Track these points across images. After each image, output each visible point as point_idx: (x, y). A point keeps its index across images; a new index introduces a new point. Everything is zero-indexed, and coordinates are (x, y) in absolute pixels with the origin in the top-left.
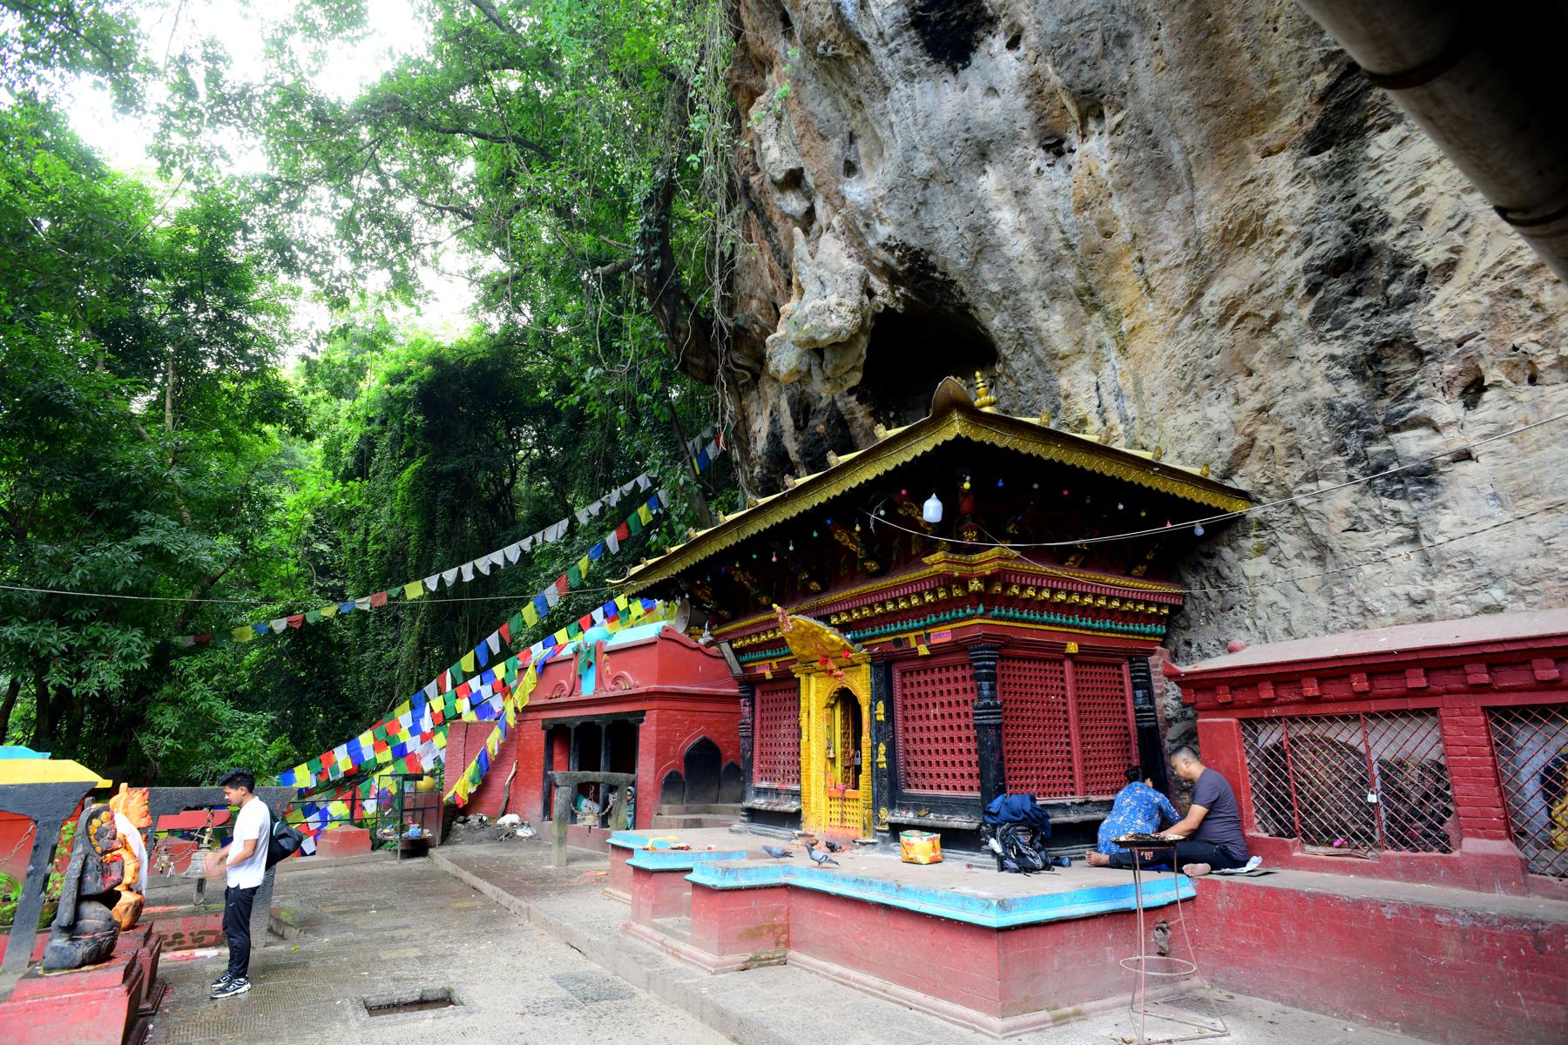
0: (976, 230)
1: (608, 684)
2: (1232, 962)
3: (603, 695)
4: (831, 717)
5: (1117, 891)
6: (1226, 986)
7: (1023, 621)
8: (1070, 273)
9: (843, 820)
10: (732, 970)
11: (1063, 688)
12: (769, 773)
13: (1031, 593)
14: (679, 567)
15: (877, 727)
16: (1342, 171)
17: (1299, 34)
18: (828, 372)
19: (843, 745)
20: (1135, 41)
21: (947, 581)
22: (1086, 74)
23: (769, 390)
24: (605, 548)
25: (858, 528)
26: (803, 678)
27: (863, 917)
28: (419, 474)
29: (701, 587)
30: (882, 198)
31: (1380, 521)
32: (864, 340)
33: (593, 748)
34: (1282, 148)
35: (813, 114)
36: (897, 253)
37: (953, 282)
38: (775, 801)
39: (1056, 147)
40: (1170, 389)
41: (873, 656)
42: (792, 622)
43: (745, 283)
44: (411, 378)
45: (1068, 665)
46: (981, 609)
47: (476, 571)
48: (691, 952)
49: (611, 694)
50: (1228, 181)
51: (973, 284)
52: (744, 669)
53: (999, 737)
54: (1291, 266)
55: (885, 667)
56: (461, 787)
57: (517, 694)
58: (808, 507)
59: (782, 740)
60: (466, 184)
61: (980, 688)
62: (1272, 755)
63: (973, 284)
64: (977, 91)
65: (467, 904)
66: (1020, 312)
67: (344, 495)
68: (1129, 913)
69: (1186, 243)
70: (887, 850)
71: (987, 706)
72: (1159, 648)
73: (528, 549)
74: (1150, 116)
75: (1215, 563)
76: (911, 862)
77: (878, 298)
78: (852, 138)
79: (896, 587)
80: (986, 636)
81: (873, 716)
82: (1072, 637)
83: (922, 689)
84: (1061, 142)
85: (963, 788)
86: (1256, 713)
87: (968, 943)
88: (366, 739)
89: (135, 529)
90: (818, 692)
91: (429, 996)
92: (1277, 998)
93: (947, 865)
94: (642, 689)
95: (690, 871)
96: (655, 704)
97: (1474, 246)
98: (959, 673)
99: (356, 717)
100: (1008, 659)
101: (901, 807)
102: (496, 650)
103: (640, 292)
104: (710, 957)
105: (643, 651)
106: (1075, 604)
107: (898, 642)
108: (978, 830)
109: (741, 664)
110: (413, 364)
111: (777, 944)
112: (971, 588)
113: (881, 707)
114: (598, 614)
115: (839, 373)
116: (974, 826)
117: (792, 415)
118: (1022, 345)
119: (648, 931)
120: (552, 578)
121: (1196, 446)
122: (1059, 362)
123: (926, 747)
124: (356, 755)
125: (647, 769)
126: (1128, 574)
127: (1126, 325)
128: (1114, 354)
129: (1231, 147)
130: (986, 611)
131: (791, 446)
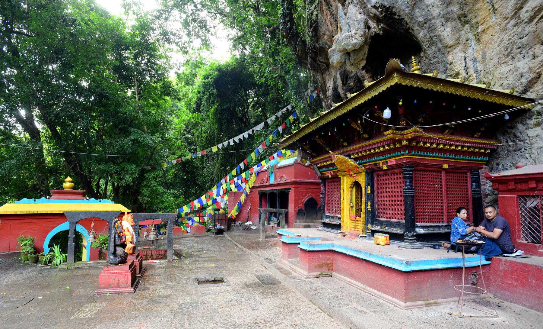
1: (278, 179)
2: (505, 290)
3: (277, 183)
4: (352, 191)
5: (456, 260)
6: (501, 298)
7: (425, 156)
9: (355, 228)
10: (312, 277)
11: (441, 182)
12: (331, 211)
13: (428, 145)
14: (297, 138)
15: (367, 195)
18: (352, 62)
19: (356, 201)
21: (394, 141)
23: (333, 71)
24: (278, 131)
25: (359, 122)
26: (342, 177)
27: (357, 263)
28: (216, 109)
29: (306, 145)
32: (367, 48)
33: (274, 200)
36: (379, 9)
37: (403, 19)
38: (332, 220)
40: (499, 56)
41: (367, 170)
42: (337, 157)
43: (322, 29)
44: (211, 77)
45: (443, 173)
46: (407, 152)
47: (234, 141)
48: (300, 270)
49: (279, 182)
51: (411, 19)
52: (322, 174)
53: (413, 200)
55: (371, 173)
56: (233, 213)
57: (249, 183)
58: (340, 114)
59: (335, 199)
60: (223, 3)
61: (406, 182)
62: (533, 211)
63: (411, 19)
65: (233, 250)
66: (432, 29)
67: (193, 118)
68: (460, 268)
70: (370, 239)
71: (409, 189)
72: (484, 166)
73: (251, 133)
75: (514, 131)
76: (378, 244)
77: (372, 30)
79: (375, 144)
80: (408, 162)
81: (366, 191)
82: (446, 162)
83: (385, 182)
85: (399, 219)
86: (527, 193)
87: (394, 276)
88: (203, 198)
89: (130, 133)
90: (347, 182)
91: (216, 279)
92: (525, 306)
93: (391, 245)
94: (289, 181)
95: (299, 244)
96: (293, 186)
98: (398, 176)
99: (202, 190)
100: (418, 171)
101: (376, 224)
102: (243, 168)
103: (283, 36)
104: (306, 273)
105: (289, 168)
106: (447, 149)
107: (375, 164)
108: (403, 234)
109: (321, 172)
110: (211, 72)
111: (329, 270)
112: (403, 144)
114: (275, 155)
115: (356, 62)
116: (402, 232)
118: (432, 42)
119: (287, 262)
120: (261, 143)
121: (510, 80)
122: (448, 49)
123: (385, 203)
124: (201, 202)
125: (291, 208)
126: (472, 137)
130: (409, 152)
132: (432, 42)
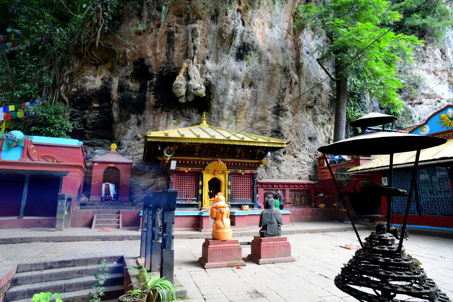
8: (235, 107)
16: (277, 119)
22: (254, 80)
35: (208, 41)
39: (243, 87)
54: (270, 128)
64: (238, 68)
66: (222, 108)
74: (258, 93)
78: (211, 53)
97: (289, 137)
113: (229, 182)
117: (118, 86)
127: (239, 121)
128: (234, 124)
131: (115, 95)
132: (218, 113)
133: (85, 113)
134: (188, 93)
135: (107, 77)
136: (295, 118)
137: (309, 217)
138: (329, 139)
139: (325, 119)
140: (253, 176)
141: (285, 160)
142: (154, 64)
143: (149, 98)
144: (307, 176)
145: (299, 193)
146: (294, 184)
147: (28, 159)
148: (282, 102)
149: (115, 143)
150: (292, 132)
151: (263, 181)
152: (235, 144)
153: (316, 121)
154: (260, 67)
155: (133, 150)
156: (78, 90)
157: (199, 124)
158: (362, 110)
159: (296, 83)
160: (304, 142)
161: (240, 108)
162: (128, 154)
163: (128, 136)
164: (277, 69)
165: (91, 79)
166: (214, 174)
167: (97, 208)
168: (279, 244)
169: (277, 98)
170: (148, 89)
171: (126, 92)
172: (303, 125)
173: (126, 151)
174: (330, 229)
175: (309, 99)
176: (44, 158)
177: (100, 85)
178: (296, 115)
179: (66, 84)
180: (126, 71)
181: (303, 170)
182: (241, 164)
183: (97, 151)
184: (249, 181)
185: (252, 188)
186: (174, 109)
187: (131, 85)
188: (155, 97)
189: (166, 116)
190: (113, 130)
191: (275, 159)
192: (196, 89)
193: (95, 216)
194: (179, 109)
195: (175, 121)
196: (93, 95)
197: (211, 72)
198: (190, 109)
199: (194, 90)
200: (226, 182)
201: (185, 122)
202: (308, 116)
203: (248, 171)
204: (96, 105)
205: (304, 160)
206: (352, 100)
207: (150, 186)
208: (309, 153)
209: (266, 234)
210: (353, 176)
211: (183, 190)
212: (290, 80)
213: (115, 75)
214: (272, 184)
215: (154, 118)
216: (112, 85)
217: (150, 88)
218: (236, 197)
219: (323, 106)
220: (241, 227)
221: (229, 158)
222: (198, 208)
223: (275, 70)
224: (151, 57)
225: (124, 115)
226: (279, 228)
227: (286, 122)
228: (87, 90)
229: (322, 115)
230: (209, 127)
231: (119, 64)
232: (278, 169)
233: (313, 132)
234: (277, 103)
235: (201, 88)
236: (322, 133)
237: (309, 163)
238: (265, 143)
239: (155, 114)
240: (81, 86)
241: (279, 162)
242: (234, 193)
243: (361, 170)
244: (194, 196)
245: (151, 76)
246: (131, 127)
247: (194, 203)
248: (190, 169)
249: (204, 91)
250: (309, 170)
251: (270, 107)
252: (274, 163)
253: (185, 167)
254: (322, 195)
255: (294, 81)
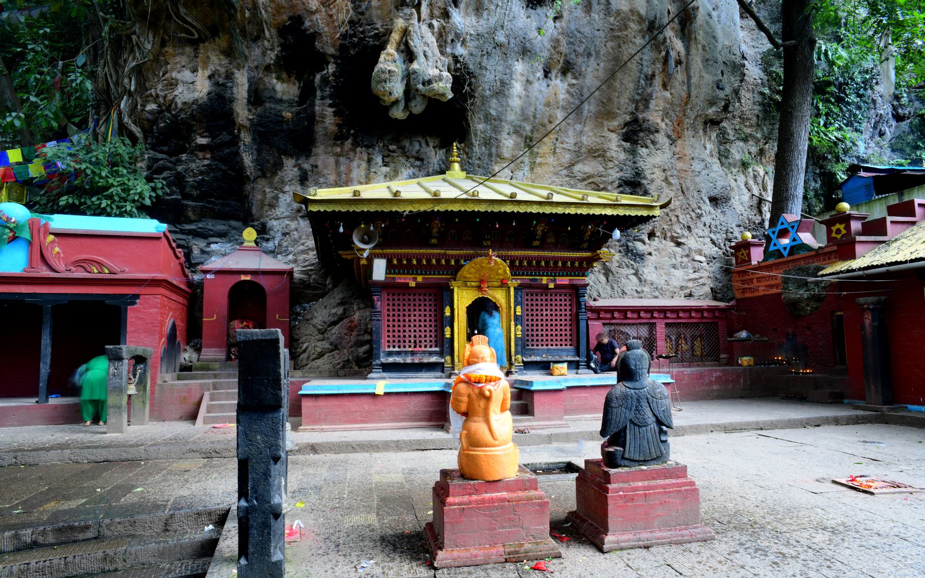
0: (503, 83)
8: (528, 128)
16: (633, 152)
17: (630, 99)
20: (592, 59)
22: (573, 56)
26: (456, 290)
30: (471, 35)
31: (628, 267)
34: (612, 131)
36: (459, 65)
39: (546, 74)
50: (596, 131)
54: (614, 175)
69: (576, 144)
74: (585, 90)
81: (515, 312)
84: (550, 72)
86: (608, 321)
105: (133, 242)
113: (519, 308)
117: (249, 91)
127: (538, 160)
128: (527, 168)
129: (599, 120)
131: (242, 113)
132: (487, 143)
133: (179, 161)
134: (409, 93)
135: (223, 70)
136: (677, 150)
137: (715, 387)
138: (761, 201)
139: (750, 153)
140: (576, 292)
141: (654, 253)
142: (326, 29)
143: (323, 117)
144: (707, 289)
145: (688, 333)
146: (676, 310)
147: (44, 268)
148: (643, 112)
149: (253, 226)
150: (669, 184)
151: (601, 303)
152: (529, 210)
153: (727, 157)
154: (589, 22)
155: (296, 241)
156: (159, 106)
157: (442, 172)
158: (847, 125)
159: (679, 62)
160: (699, 208)
161: (542, 129)
162: (286, 251)
163: (282, 210)
164: (632, 25)
165: (184, 79)
166: (479, 288)
167: (215, 376)
168: (664, 487)
169: (633, 100)
170: (318, 93)
171: (268, 105)
172: (697, 166)
173: (280, 245)
174: (778, 421)
175: (712, 103)
176: (79, 264)
177: (205, 91)
178: (679, 142)
179: (130, 94)
180: (264, 54)
181: (696, 275)
182: (547, 263)
183: (213, 246)
184: (568, 303)
185: (576, 320)
186: (383, 140)
187: (279, 87)
188: (335, 114)
189: (366, 158)
190: (247, 197)
191: (628, 251)
192: (429, 82)
193: (207, 395)
194: (396, 140)
195: (388, 169)
196: (192, 116)
197: (464, 39)
198: (420, 139)
199: (424, 84)
200: (510, 307)
201: (411, 171)
202: (708, 146)
203: (564, 280)
204: (202, 141)
205: (700, 252)
206: (822, 100)
207: (334, 323)
208: (712, 235)
209: (623, 458)
210: (832, 286)
211: (407, 329)
212: (663, 53)
213: (239, 65)
214: (624, 311)
215: (337, 163)
216: (235, 90)
217: (322, 91)
218: (535, 343)
219: (743, 119)
220: (549, 419)
221: (516, 248)
222: (443, 372)
223: (626, 27)
224: (316, 11)
225: (268, 161)
226: (663, 438)
227: (654, 160)
228: (180, 105)
229: (741, 144)
230: (467, 178)
231: (244, 37)
232: (636, 274)
233: (720, 183)
234: (632, 113)
235: (440, 78)
236: (743, 187)
237: (711, 259)
238: (605, 206)
239: (339, 155)
240: (166, 96)
241: (639, 257)
242: (530, 333)
243: (860, 269)
244: (433, 344)
245: (321, 60)
246: (287, 188)
247: (434, 359)
248: (420, 279)
249: (449, 86)
250: (712, 275)
251: (615, 123)
252: (627, 261)
253: (408, 274)
254: (744, 334)
255: (673, 54)
